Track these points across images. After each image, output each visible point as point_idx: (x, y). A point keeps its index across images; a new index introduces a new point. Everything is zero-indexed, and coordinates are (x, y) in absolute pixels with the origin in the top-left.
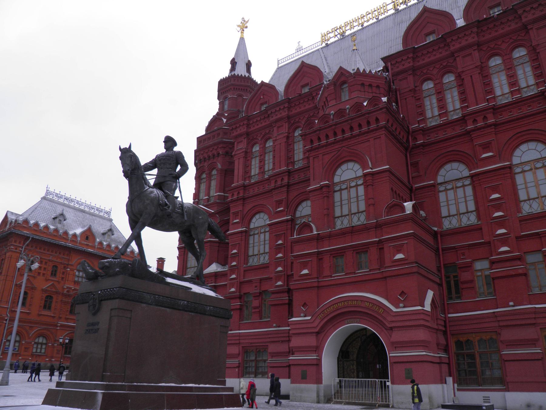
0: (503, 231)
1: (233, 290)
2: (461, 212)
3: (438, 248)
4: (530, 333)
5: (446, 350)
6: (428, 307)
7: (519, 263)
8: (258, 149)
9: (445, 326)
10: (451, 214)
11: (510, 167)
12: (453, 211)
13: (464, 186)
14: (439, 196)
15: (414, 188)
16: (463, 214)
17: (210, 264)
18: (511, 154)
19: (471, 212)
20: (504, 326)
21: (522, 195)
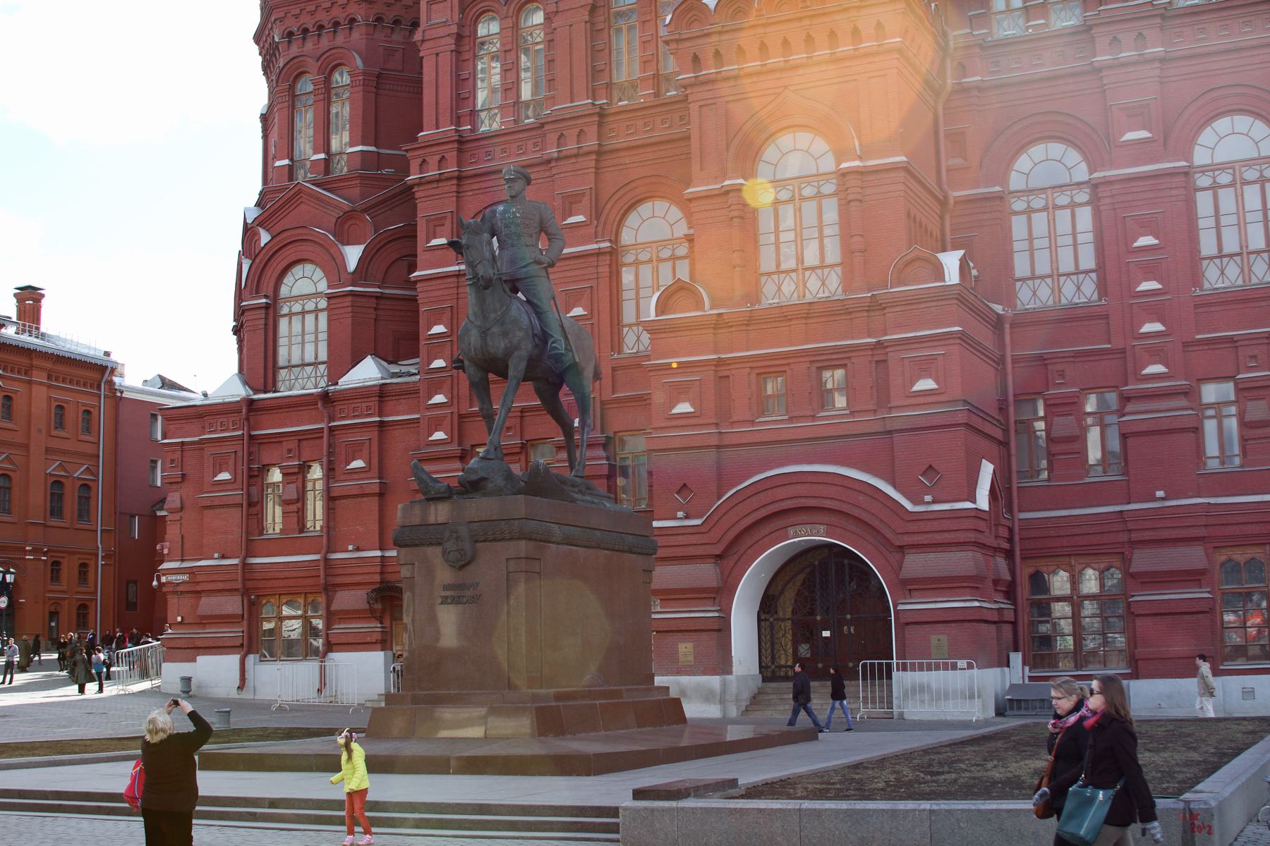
0: (1157, 327)
1: (439, 435)
2: (1061, 271)
3: (1003, 357)
4: (1193, 557)
5: (1010, 592)
6: (983, 502)
7: (1183, 402)
8: (494, 27)
9: (1010, 540)
10: (1037, 273)
11: (1187, 173)
12: (1043, 267)
13: (1073, 206)
14: (1010, 227)
15: (952, 201)
16: (1068, 275)
17: (356, 361)
18: (1191, 142)
19: (1087, 272)
20: (1140, 542)
21: (1207, 245)
